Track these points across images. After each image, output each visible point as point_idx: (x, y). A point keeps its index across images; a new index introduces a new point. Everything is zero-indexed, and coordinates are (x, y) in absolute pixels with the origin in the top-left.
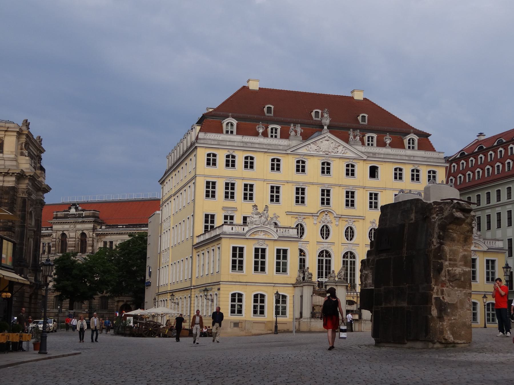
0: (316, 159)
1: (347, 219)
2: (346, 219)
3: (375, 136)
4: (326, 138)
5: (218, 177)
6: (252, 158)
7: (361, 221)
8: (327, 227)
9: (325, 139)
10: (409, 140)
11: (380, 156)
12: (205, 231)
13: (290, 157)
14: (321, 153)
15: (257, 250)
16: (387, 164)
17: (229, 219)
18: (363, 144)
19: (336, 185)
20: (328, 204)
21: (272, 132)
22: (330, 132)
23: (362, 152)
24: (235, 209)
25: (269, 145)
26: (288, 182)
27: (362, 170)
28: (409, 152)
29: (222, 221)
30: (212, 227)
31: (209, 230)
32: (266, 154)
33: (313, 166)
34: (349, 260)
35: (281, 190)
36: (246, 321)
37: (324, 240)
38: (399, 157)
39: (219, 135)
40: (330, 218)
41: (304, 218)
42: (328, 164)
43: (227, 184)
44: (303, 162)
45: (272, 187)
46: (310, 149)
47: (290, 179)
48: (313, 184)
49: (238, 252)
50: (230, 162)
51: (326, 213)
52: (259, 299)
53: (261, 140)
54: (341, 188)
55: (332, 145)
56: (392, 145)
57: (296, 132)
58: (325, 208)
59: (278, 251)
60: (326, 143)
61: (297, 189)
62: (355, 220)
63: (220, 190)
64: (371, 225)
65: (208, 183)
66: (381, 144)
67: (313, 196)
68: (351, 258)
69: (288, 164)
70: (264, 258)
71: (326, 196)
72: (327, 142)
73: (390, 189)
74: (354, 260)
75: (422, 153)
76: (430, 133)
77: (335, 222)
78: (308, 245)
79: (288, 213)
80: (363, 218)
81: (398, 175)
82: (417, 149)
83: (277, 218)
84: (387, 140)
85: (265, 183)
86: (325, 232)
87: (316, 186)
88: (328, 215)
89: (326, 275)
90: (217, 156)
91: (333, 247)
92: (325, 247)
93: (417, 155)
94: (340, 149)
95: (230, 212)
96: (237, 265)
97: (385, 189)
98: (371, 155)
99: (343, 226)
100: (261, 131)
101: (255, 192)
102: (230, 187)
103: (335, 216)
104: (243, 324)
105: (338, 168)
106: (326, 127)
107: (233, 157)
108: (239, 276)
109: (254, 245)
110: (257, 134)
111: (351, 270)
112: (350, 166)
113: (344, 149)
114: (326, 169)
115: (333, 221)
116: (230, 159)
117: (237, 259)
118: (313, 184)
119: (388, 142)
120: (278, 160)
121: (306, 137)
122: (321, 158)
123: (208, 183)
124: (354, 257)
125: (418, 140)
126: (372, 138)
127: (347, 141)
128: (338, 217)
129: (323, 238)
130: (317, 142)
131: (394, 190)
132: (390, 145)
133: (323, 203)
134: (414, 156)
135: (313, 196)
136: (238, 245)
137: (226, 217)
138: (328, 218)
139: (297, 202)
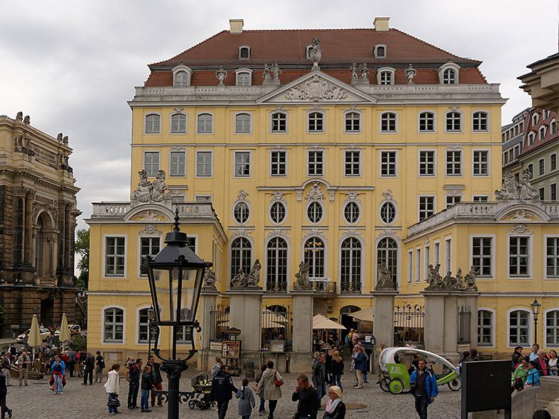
0: (300, 110)
1: (348, 192)
3: (392, 70)
4: (316, 78)
5: (436, 145)
6: (392, 116)
8: (318, 205)
9: (314, 79)
11: (397, 98)
12: (421, 220)
13: (263, 110)
14: (307, 100)
15: (145, 242)
17: (453, 200)
18: (373, 81)
20: (320, 172)
21: (383, 79)
22: (322, 69)
23: (369, 94)
24: (462, 187)
25: (232, 96)
28: (443, 88)
29: (444, 205)
30: (430, 214)
31: (426, 217)
32: (228, 110)
33: (297, 120)
34: (351, 250)
35: (397, 157)
39: (215, 88)
41: (284, 195)
42: (320, 116)
43: (449, 154)
44: (283, 116)
45: (384, 154)
46: (292, 97)
47: (262, 141)
48: (296, 145)
50: (453, 123)
51: (316, 185)
53: (221, 90)
56: (417, 81)
58: (315, 177)
59: (110, 241)
60: (316, 85)
61: (274, 154)
63: (440, 162)
64: (383, 198)
65: (423, 154)
66: (401, 81)
67: (297, 164)
68: (354, 246)
70: (489, 254)
71: (316, 162)
72: (316, 84)
74: (359, 249)
75: (465, 88)
79: (261, 189)
80: (371, 189)
81: (426, 123)
83: (245, 196)
84: (409, 73)
86: (315, 212)
87: (300, 149)
89: (317, 272)
90: (435, 116)
91: (325, 233)
92: (314, 232)
93: (456, 92)
95: (177, 192)
97: (405, 145)
98: (384, 97)
99: (342, 203)
100: (221, 77)
101: (270, 163)
102: (454, 158)
105: (334, 120)
106: (316, 64)
107: (457, 115)
110: (216, 83)
111: (280, 264)
112: (388, 115)
113: (342, 92)
114: (316, 123)
116: (453, 118)
117: (116, 256)
118: (296, 145)
119: (411, 76)
120: (392, 116)
121: (284, 80)
123: (476, 153)
124: (359, 246)
127: (349, 82)
128: (333, 190)
130: (302, 86)
131: (419, 145)
133: (311, 172)
135: (297, 164)
137: (449, 200)
138: (318, 192)
139: (274, 172)
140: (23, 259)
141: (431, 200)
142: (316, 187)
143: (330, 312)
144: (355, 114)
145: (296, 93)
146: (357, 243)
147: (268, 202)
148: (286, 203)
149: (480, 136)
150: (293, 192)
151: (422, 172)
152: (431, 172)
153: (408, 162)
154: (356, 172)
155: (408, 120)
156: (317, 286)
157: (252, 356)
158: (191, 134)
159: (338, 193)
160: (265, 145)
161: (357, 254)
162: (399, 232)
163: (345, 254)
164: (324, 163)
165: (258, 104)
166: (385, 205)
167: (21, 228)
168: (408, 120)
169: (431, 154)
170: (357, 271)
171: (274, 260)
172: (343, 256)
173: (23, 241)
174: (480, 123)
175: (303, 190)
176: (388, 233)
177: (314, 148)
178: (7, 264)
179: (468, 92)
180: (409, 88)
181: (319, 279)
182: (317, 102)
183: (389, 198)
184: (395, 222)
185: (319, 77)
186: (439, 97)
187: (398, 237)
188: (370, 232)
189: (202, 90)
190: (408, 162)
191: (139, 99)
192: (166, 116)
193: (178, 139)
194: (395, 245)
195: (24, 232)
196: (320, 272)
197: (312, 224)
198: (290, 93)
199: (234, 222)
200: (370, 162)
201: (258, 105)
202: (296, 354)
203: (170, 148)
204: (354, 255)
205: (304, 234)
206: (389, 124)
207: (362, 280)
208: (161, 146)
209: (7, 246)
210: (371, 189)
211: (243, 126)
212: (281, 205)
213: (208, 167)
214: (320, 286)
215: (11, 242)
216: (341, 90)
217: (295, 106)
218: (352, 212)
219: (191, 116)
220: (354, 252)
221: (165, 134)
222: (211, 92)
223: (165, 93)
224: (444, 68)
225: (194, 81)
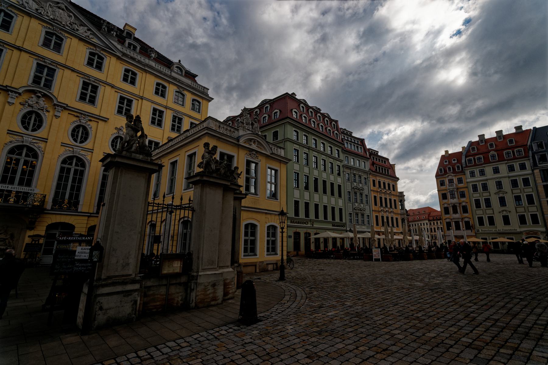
1: (78, 115)
2: (78, 115)
7: (101, 123)
16: (148, 75)
40: (42, 102)
51: (40, 95)
62: (92, 119)
64: (115, 131)
72: (61, 11)
74: (82, 169)
81: (160, 91)
91: (42, 145)
97: (142, 98)
103: (55, 102)
115: (50, 109)
122: (45, 25)
128: (61, 107)
131: (153, 102)
132: (154, 59)
138: (42, 102)
142: (39, 97)
143: (32, 229)
163: (64, 172)
169: (161, 112)
175: (20, 94)
177: (45, 62)
180: (150, 62)
181: (24, 189)
205: (12, 139)
207: (81, 198)
217: (30, 15)
218: (80, 133)
220: (76, 171)
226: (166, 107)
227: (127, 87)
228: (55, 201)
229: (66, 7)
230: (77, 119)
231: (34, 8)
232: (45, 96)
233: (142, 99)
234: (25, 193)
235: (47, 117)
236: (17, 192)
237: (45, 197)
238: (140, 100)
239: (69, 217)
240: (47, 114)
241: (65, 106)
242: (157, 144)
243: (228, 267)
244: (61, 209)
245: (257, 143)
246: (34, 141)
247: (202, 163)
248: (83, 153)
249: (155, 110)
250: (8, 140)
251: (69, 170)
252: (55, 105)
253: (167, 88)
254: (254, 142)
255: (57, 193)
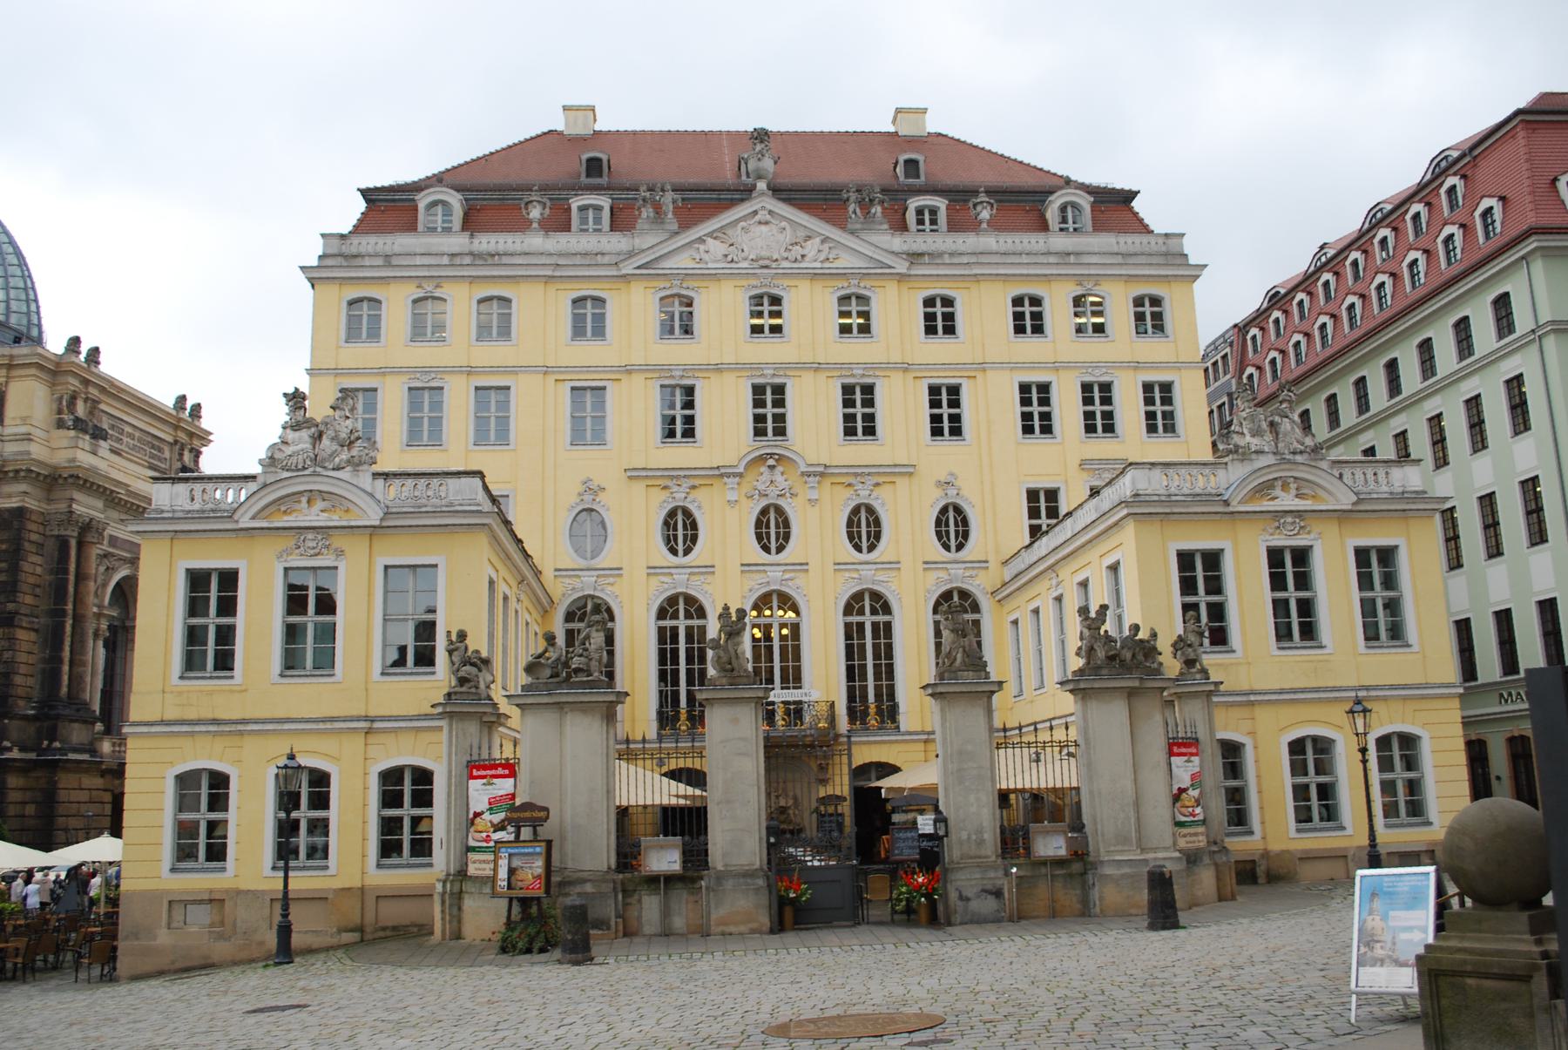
1: (851, 480)
2: (851, 480)
3: (941, 203)
8: (780, 511)
9: (757, 218)
10: (1063, 209)
11: (956, 260)
14: (745, 264)
16: (985, 287)
19: (802, 367)
20: (780, 431)
26: (628, 370)
27: (896, 311)
28: (1059, 242)
32: (552, 288)
33: (723, 311)
34: (868, 619)
36: (238, 892)
37: (773, 558)
38: (1025, 259)
46: (706, 257)
47: (636, 359)
48: (718, 369)
49: (213, 593)
51: (771, 462)
52: (303, 793)
53: (535, 241)
54: (822, 376)
55: (781, 237)
57: (658, 208)
58: (769, 444)
60: (764, 231)
62: (881, 480)
64: (938, 493)
68: (874, 612)
69: (634, 313)
72: (763, 228)
73: (1001, 366)
75: (1107, 241)
76: (1135, 189)
77: (805, 493)
78: (710, 578)
79: (635, 475)
80: (906, 471)
82: (1090, 229)
84: (979, 208)
85: (551, 379)
86: (772, 529)
87: (729, 378)
88: (780, 469)
89: (784, 679)
91: (801, 580)
93: (1090, 249)
94: (811, 248)
96: (210, 649)
97: (983, 367)
100: (535, 213)
103: (804, 469)
104: (227, 904)
105: (811, 312)
106: (762, 185)
108: (211, 693)
109: (279, 557)
110: (523, 226)
113: (826, 246)
118: (718, 369)
119: (985, 214)
122: (745, 283)
124: (887, 609)
125: (1094, 205)
126: (934, 212)
127: (841, 224)
129: (766, 549)
130: (730, 232)
131: (1014, 366)
132: (989, 223)
133: (759, 432)
134: (1077, 254)
136: (213, 559)
138: (779, 478)
140: (64, 690)
141: (1052, 495)
142: (772, 467)
143: (824, 782)
144: (859, 297)
145: (716, 248)
146: (881, 604)
147: (649, 509)
148: (699, 507)
149: (1152, 348)
150: (715, 482)
151: (1028, 430)
152: (1047, 429)
153: (991, 407)
154: (870, 431)
155: (984, 313)
156: (787, 712)
157: (589, 888)
158: (460, 340)
159: (827, 482)
160: (646, 369)
161: (884, 631)
162: (982, 573)
164: (792, 410)
165: (624, 272)
166: (944, 510)
167: (64, 613)
168: (984, 313)
169: (1044, 388)
170: (886, 671)
171: (675, 652)
172: (848, 636)
173: (67, 649)
174: (1150, 316)
175: (741, 475)
176: (955, 575)
178: (21, 703)
179: (1116, 249)
181: (792, 695)
182: (767, 267)
183: (952, 492)
184: (973, 550)
185: (770, 212)
186: (1052, 259)
187: (979, 585)
188: (911, 575)
189: (486, 242)
190: (991, 407)
191: (329, 262)
192: (396, 305)
193: (425, 355)
194: (976, 608)
195: (69, 622)
196: (793, 677)
197: (763, 557)
198: (702, 247)
199: (569, 559)
200: (904, 409)
201: (624, 276)
202: (720, 877)
203: (405, 378)
204: (876, 635)
206: (940, 319)
208: (382, 372)
209: (22, 657)
210: (906, 471)
211: (588, 318)
212: (687, 513)
213: (503, 423)
214: (795, 711)
215: (35, 649)
216: (823, 242)
217: (715, 277)
218: (864, 528)
219: (460, 304)
220: (875, 625)
221: (395, 344)
222: (510, 247)
223: (397, 249)
224: (1056, 201)
225: (471, 223)
226: (1056, 367)
227: (940, 349)
228: (851, 712)
229: (770, 212)
230: (850, 491)
231: (720, 256)
232: (781, 459)
233: (984, 370)
234: (795, 703)
235: (792, 508)
236: (785, 703)
237: (832, 705)
238: (979, 375)
239: (885, 747)
240: (796, 502)
241: (821, 469)
242: (1052, 495)
243: (1166, 849)
244: (866, 728)
245: (1293, 486)
246: (787, 576)
247: (1080, 648)
248: (881, 576)
249: (1025, 388)
250: (746, 588)
251: (861, 626)
252: (803, 474)
253: (1047, 304)
254: (1285, 487)
255: (851, 698)
